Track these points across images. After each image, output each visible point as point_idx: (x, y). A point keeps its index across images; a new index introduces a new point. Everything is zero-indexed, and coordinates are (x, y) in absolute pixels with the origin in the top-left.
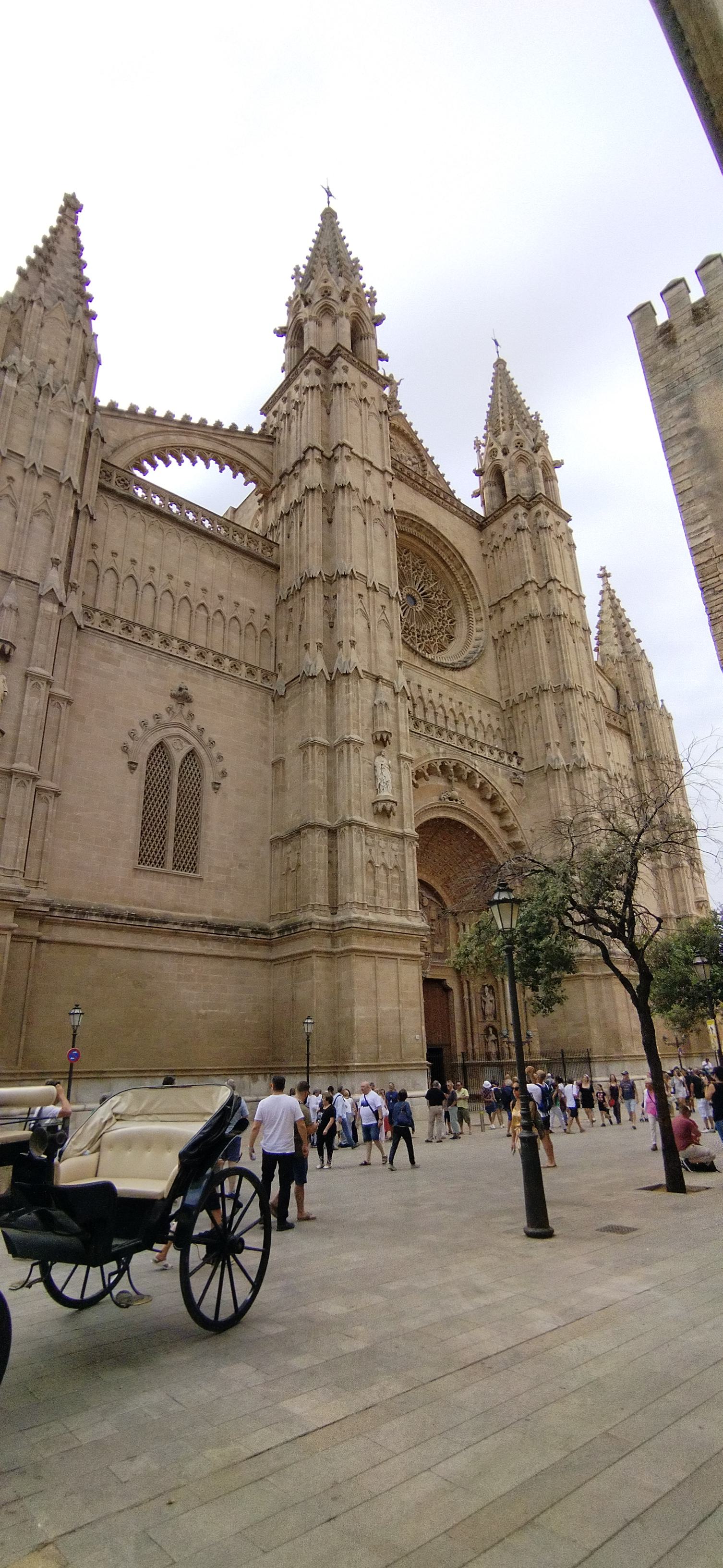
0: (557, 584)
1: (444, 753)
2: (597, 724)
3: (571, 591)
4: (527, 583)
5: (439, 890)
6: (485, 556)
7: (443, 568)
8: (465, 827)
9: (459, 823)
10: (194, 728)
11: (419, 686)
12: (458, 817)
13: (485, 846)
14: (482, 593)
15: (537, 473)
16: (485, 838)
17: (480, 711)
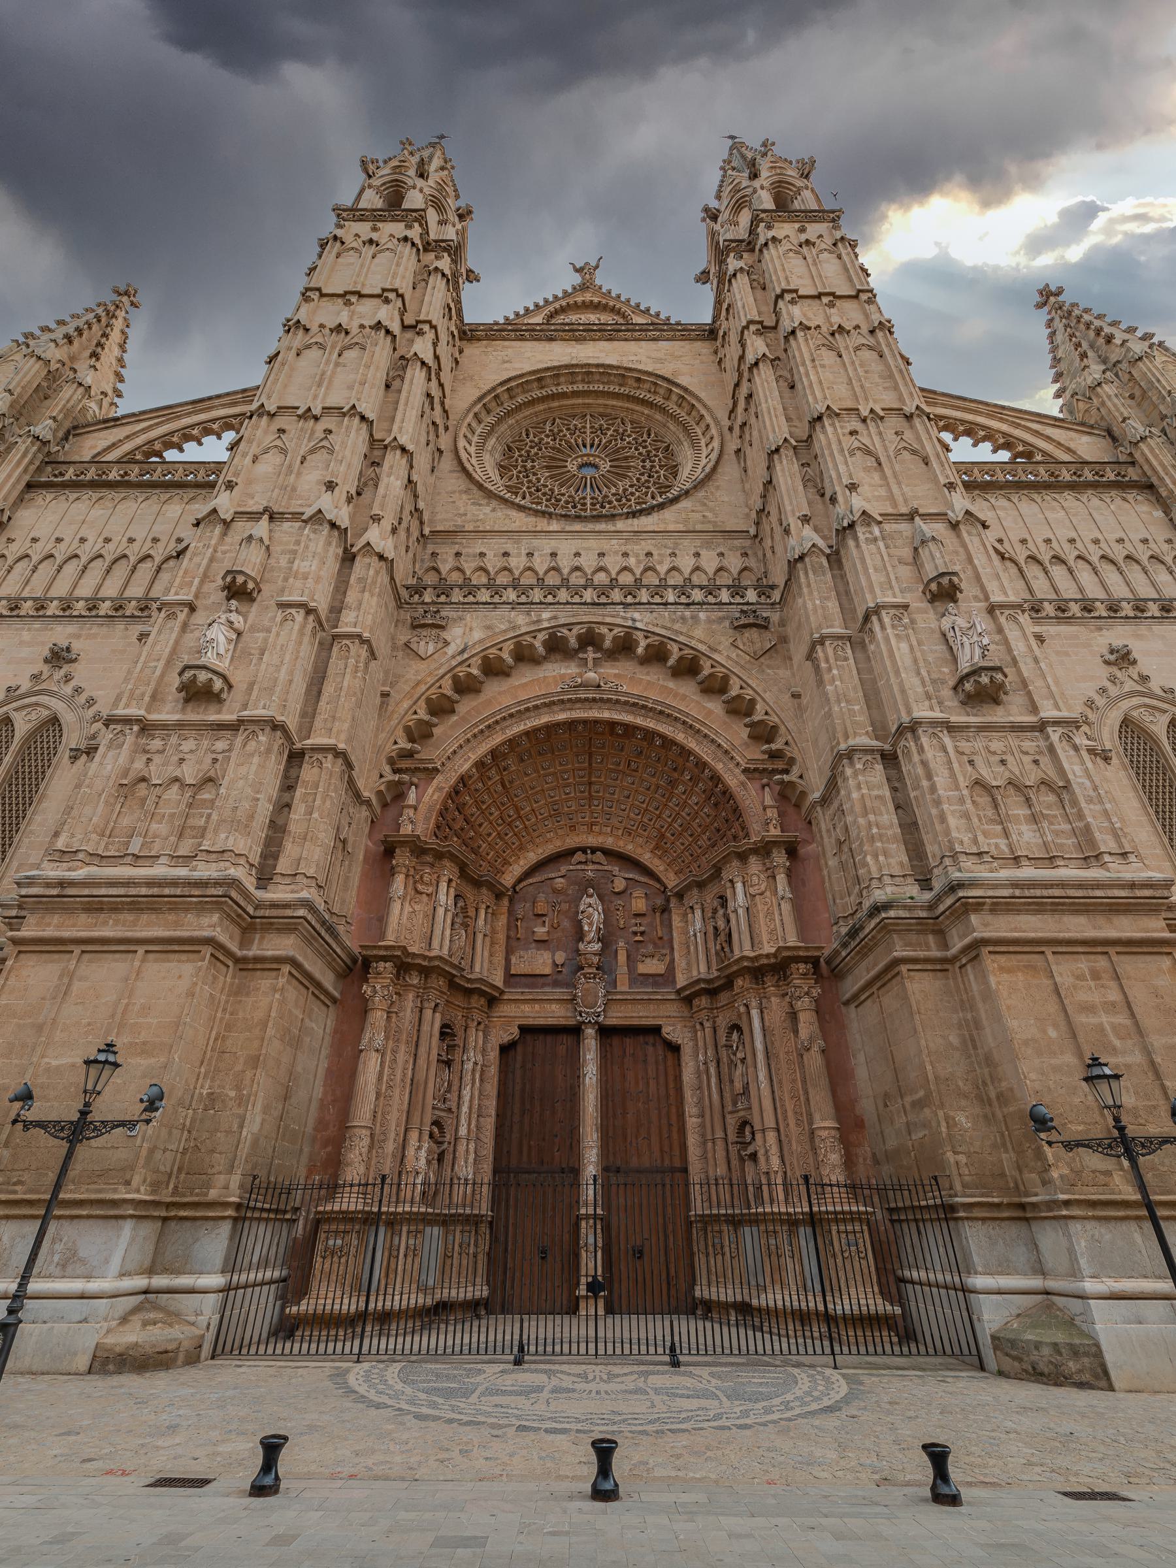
0: (788, 297)
1: (555, 618)
2: (914, 452)
3: (833, 294)
4: (742, 333)
5: (646, 858)
6: (720, 362)
7: (646, 412)
8: (630, 730)
9: (612, 724)
10: (68, 689)
11: (554, 555)
12: (606, 715)
13: (685, 752)
14: (709, 403)
15: (760, 197)
16: (680, 737)
17: (697, 555)
